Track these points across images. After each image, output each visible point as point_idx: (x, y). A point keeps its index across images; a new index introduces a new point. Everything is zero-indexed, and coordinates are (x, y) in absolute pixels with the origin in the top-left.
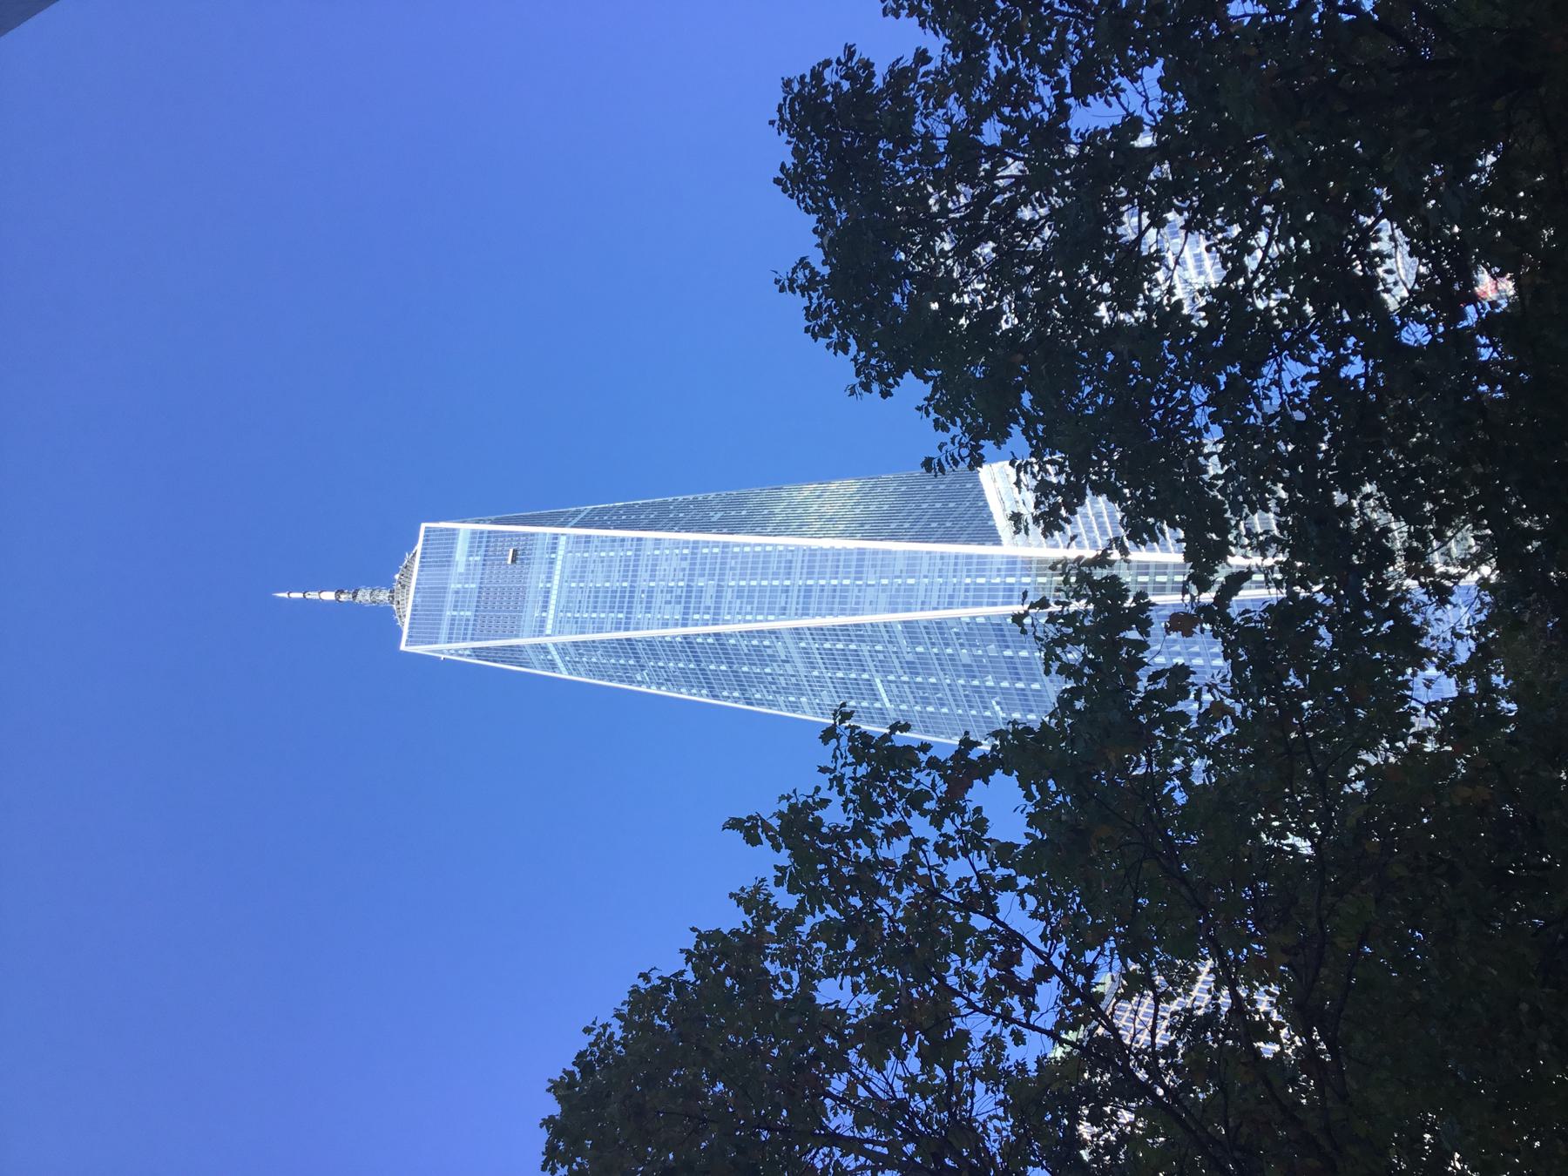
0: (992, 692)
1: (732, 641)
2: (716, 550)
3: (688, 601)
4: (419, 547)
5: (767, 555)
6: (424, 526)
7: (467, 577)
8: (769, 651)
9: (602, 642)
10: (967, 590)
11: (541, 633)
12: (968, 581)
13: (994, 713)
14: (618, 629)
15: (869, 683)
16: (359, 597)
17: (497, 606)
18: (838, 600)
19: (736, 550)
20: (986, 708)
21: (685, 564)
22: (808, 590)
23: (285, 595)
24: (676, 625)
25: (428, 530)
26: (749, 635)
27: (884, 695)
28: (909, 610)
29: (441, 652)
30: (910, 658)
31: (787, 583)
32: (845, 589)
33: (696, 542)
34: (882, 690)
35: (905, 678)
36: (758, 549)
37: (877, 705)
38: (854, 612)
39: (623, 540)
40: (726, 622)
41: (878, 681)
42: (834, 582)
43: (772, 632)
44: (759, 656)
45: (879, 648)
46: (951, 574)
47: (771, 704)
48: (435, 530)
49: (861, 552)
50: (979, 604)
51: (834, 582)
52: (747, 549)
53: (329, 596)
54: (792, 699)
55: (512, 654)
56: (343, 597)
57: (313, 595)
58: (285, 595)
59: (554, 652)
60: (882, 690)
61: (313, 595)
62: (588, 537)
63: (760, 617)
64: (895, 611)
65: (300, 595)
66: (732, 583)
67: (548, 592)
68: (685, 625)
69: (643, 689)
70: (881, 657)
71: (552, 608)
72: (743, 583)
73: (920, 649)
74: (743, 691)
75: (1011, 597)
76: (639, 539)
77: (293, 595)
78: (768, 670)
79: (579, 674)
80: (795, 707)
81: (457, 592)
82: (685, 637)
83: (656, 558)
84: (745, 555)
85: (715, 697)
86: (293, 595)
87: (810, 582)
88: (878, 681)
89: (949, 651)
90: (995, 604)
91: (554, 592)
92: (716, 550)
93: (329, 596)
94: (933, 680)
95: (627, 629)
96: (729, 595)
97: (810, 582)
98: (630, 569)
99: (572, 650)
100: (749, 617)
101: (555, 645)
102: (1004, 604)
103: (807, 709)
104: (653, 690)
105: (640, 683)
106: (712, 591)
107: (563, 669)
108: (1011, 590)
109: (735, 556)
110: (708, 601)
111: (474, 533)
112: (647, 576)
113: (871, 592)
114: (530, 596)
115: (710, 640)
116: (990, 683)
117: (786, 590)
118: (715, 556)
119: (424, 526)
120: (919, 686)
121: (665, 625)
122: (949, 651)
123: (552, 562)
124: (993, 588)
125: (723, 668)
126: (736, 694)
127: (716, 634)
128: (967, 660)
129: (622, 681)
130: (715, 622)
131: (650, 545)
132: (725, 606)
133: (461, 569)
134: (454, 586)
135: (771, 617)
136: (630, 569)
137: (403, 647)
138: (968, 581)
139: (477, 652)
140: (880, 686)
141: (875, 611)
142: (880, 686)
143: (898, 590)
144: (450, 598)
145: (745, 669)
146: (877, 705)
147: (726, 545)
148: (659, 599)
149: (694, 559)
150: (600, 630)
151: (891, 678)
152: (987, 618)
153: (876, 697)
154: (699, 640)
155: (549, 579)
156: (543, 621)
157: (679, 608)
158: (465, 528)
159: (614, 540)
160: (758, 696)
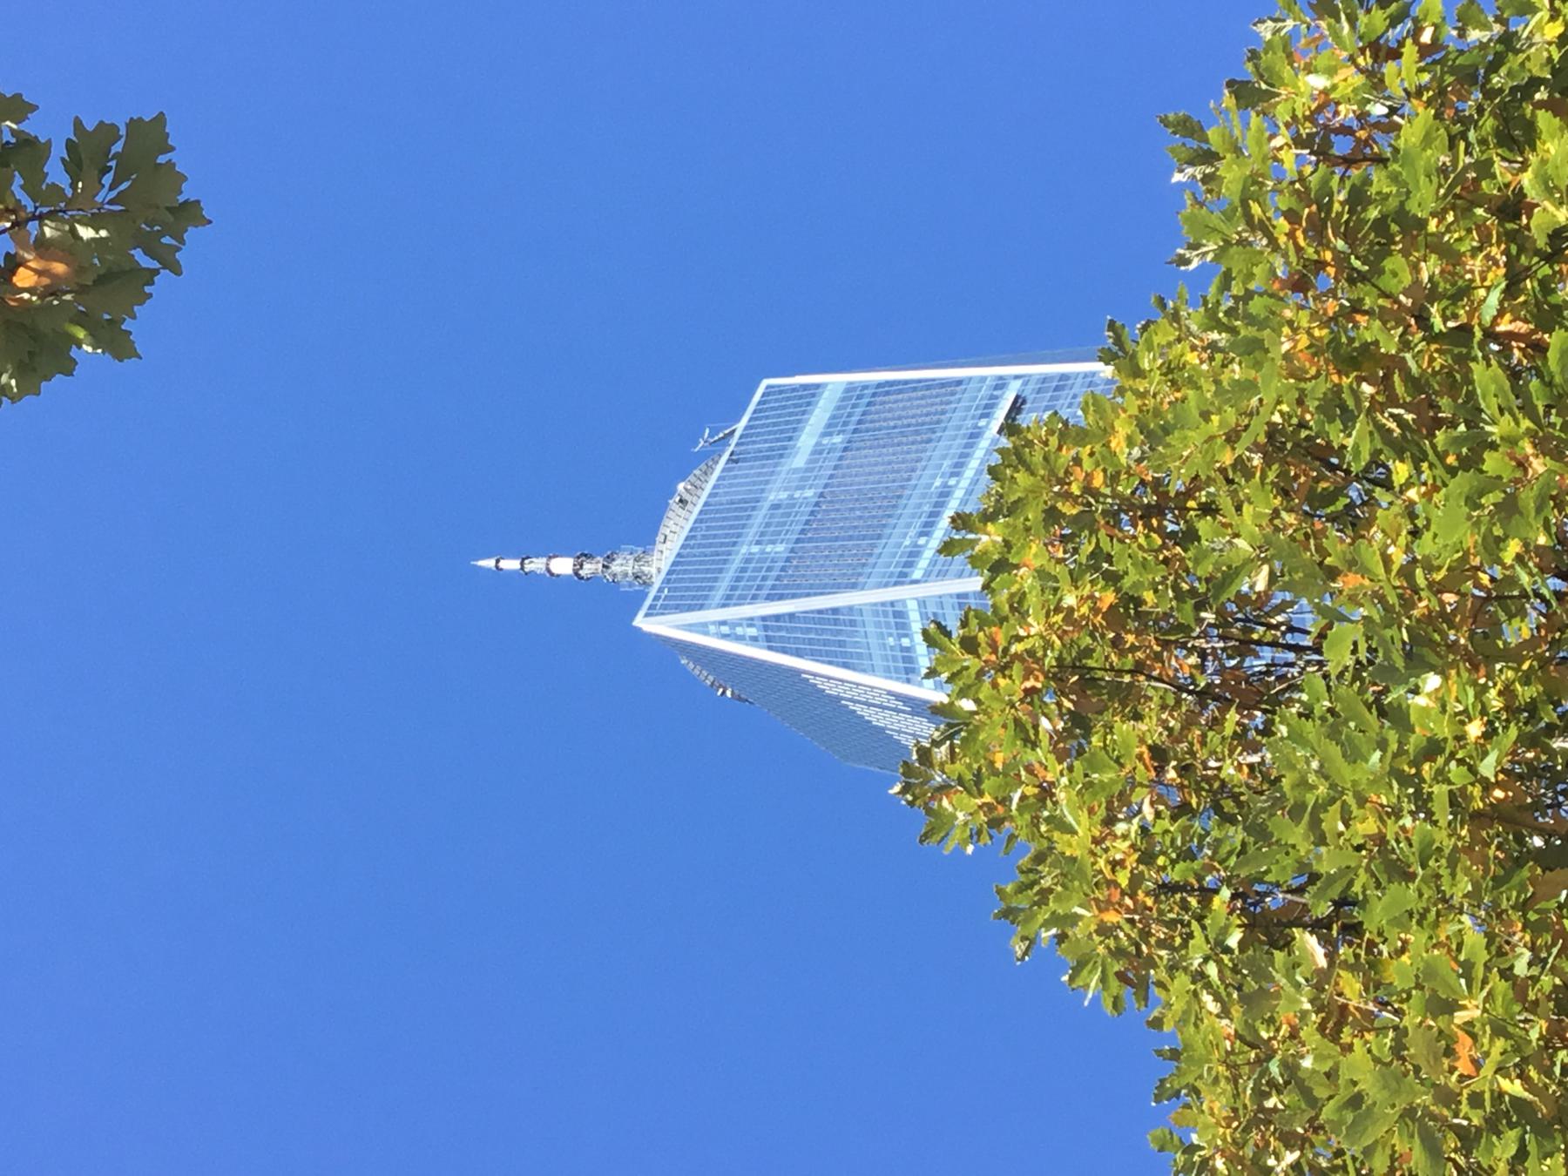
6: (766, 382)
7: (803, 480)
11: (902, 578)
16: (616, 567)
23: (489, 563)
29: (702, 628)
48: (781, 390)
53: (563, 566)
56: (588, 569)
57: (536, 565)
58: (489, 563)
61: (536, 565)
62: (1064, 377)
67: (946, 493)
77: (505, 564)
81: (775, 507)
86: (505, 564)
91: (959, 494)
93: (563, 566)
101: (922, 603)
111: (850, 388)
114: (915, 503)
123: (976, 435)
133: (799, 461)
134: (772, 497)
137: (642, 622)
139: (773, 631)
144: (759, 517)
155: (958, 469)
156: (915, 553)
158: (836, 381)
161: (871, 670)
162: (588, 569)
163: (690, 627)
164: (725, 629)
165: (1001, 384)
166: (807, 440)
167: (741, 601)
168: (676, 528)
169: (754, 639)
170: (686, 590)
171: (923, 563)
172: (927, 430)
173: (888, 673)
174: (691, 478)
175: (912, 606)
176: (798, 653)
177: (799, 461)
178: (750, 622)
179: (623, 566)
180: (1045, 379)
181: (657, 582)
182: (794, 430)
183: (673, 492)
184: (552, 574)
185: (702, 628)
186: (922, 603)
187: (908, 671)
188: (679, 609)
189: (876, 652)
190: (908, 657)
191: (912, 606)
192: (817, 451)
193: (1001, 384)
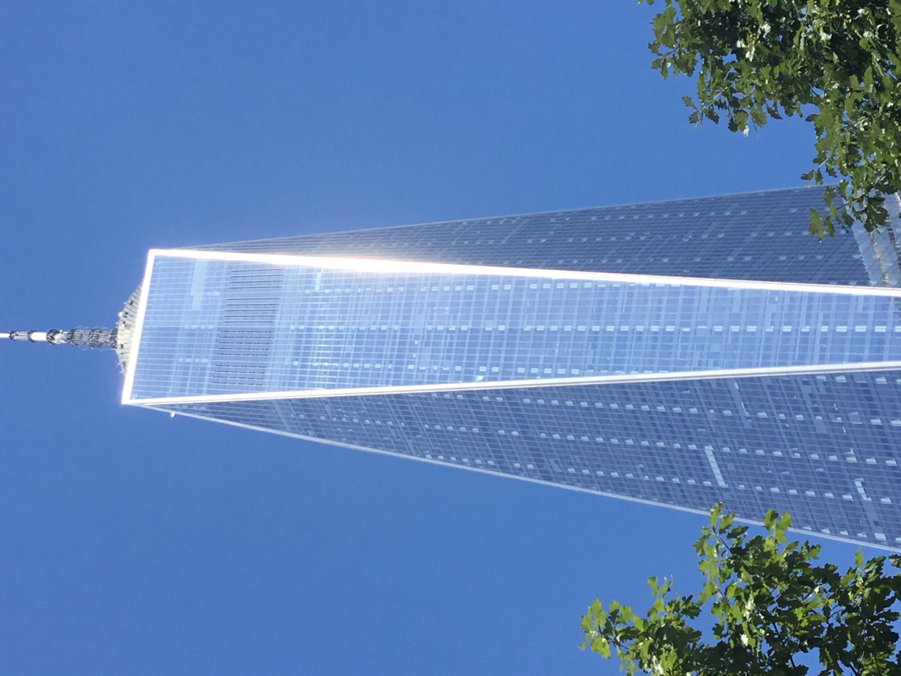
0: (858, 470)
2: (507, 287)
5: (571, 292)
6: (153, 254)
10: (824, 341)
12: (825, 329)
13: (858, 496)
15: (698, 456)
19: (533, 286)
20: (847, 490)
25: (157, 259)
27: (717, 471)
34: (714, 465)
36: (560, 286)
37: (707, 483)
42: (655, 328)
46: (803, 320)
48: (165, 259)
49: (690, 290)
50: (840, 360)
52: (547, 286)
53: (40, 336)
56: (59, 338)
57: (22, 336)
60: (714, 465)
61: (22, 336)
65: (7, 335)
66: (528, 328)
74: (539, 463)
75: (880, 350)
85: (505, 469)
90: (859, 359)
92: (507, 287)
93: (40, 336)
102: (870, 359)
108: (882, 342)
109: (532, 293)
115: (500, 399)
116: (853, 460)
119: (153, 254)
120: (762, 461)
124: (858, 339)
126: (530, 466)
127: (507, 391)
128: (822, 430)
135: (575, 371)
138: (825, 329)
139: (214, 408)
140: (712, 459)
142: (712, 459)
146: (707, 483)
147: (520, 281)
152: (850, 376)
161: (284, 429)
164: (186, 408)
169: (203, 412)
174: (126, 310)
183: (118, 319)
184: (33, 341)
189: (284, 421)
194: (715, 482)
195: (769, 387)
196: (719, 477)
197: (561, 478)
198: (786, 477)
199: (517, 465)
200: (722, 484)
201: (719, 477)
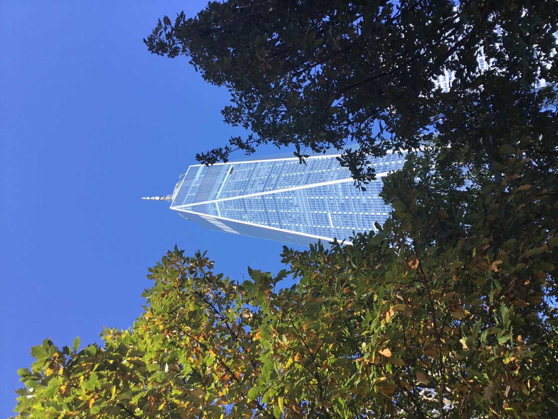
1: (278, 198)
3: (267, 184)
4: (186, 174)
8: (291, 202)
9: (234, 201)
11: (215, 199)
14: (240, 195)
15: (326, 215)
16: (167, 198)
17: (205, 191)
18: (320, 178)
21: (269, 170)
22: (310, 174)
23: (144, 198)
24: (260, 191)
26: (284, 194)
28: (345, 178)
29: (181, 208)
30: (343, 202)
31: (303, 173)
32: (323, 173)
33: (275, 162)
35: (340, 213)
37: (328, 227)
38: (324, 181)
39: (251, 164)
40: (277, 189)
41: (329, 214)
43: (293, 192)
44: (288, 204)
45: (331, 198)
47: (289, 228)
48: (193, 167)
51: (320, 171)
53: (157, 198)
54: (297, 225)
55: (203, 209)
56: (162, 198)
57: (153, 198)
58: (144, 198)
59: (217, 207)
61: (153, 198)
63: (290, 186)
64: (339, 179)
67: (221, 184)
68: (263, 191)
69: (245, 223)
70: (332, 202)
71: (221, 189)
72: (287, 175)
73: (347, 197)
76: (257, 163)
78: (290, 211)
79: (225, 217)
80: (297, 229)
82: (262, 196)
83: (260, 169)
84: (291, 164)
85: (270, 225)
87: (311, 172)
88: (329, 214)
89: (358, 197)
91: (223, 184)
93: (157, 198)
94: (350, 213)
95: (243, 195)
96: (281, 179)
97: (311, 172)
98: (250, 174)
99: (223, 205)
100: (286, 187)
101: (218, 203)
103: (302, 230)
104: (249, 223)
105: (245, 220)
106: (276, 179)
107: (219, 214)
109: (287, 165)
110: (274, 182)
112: (255, 175)
113: (332, 173)
114: (216, 186)
115: (271, 198)
117: (301, 175)
118: (280, 166)
120: (345, 216)
121: (256, 192)
122: (358, 197)
123: (226, 174)
125: (274, 211)
126: (277, 224)
127: (273, 194)
129: (238, 219)
130: (274, 189)
131: (259, 165)
132: (279, 183)
133: (197, 179)
134: (193, 185)
135: (294, 186)
136: (250, 174)
137: (171, 208)
139: (193, 208)
141: (332, 180)
143: (343, 171)
144: (191, 189)
145: (282, 211)
146: (328, 227)
147: (285, 162)
148: (257, 182)
149: (273, 169)
150: (234, 196)
151: (335, 213)
153: (328, 224)
154: (267, 198)
156: (217, 194)
157: (263, 185)
159: (248, 164)
160: (285, 224)
161: (210, 214)
162: (162, 198)
163: (179, 208)
165: (230, 165)
166: (198, 176)
167: (188, 203)
168: (176, 191)
170: (179, 201)
171: (218, 196)
172: (218, 174)
173: (213, 214)
175: (217, 203)
176: (198, 212)
177: (197, 179)
178: (190, 207)
179: (168, 198)
180: (237, 164)
181: (174, 200)
182: (195, 174)
185: (181, 208)
186: (218, 203)
187: (217, 214)
188: (177, 205)
190: (216, 212)
191: (217, 203)
192: (200, 178)
193: (230, 165)
194: (330, 226)
195: (350, 186)
196: (331, 224)
197: (285, 228)
198: (352, 222)
199: (273, 224)
200: (332, 226)
201: (331, 224)
